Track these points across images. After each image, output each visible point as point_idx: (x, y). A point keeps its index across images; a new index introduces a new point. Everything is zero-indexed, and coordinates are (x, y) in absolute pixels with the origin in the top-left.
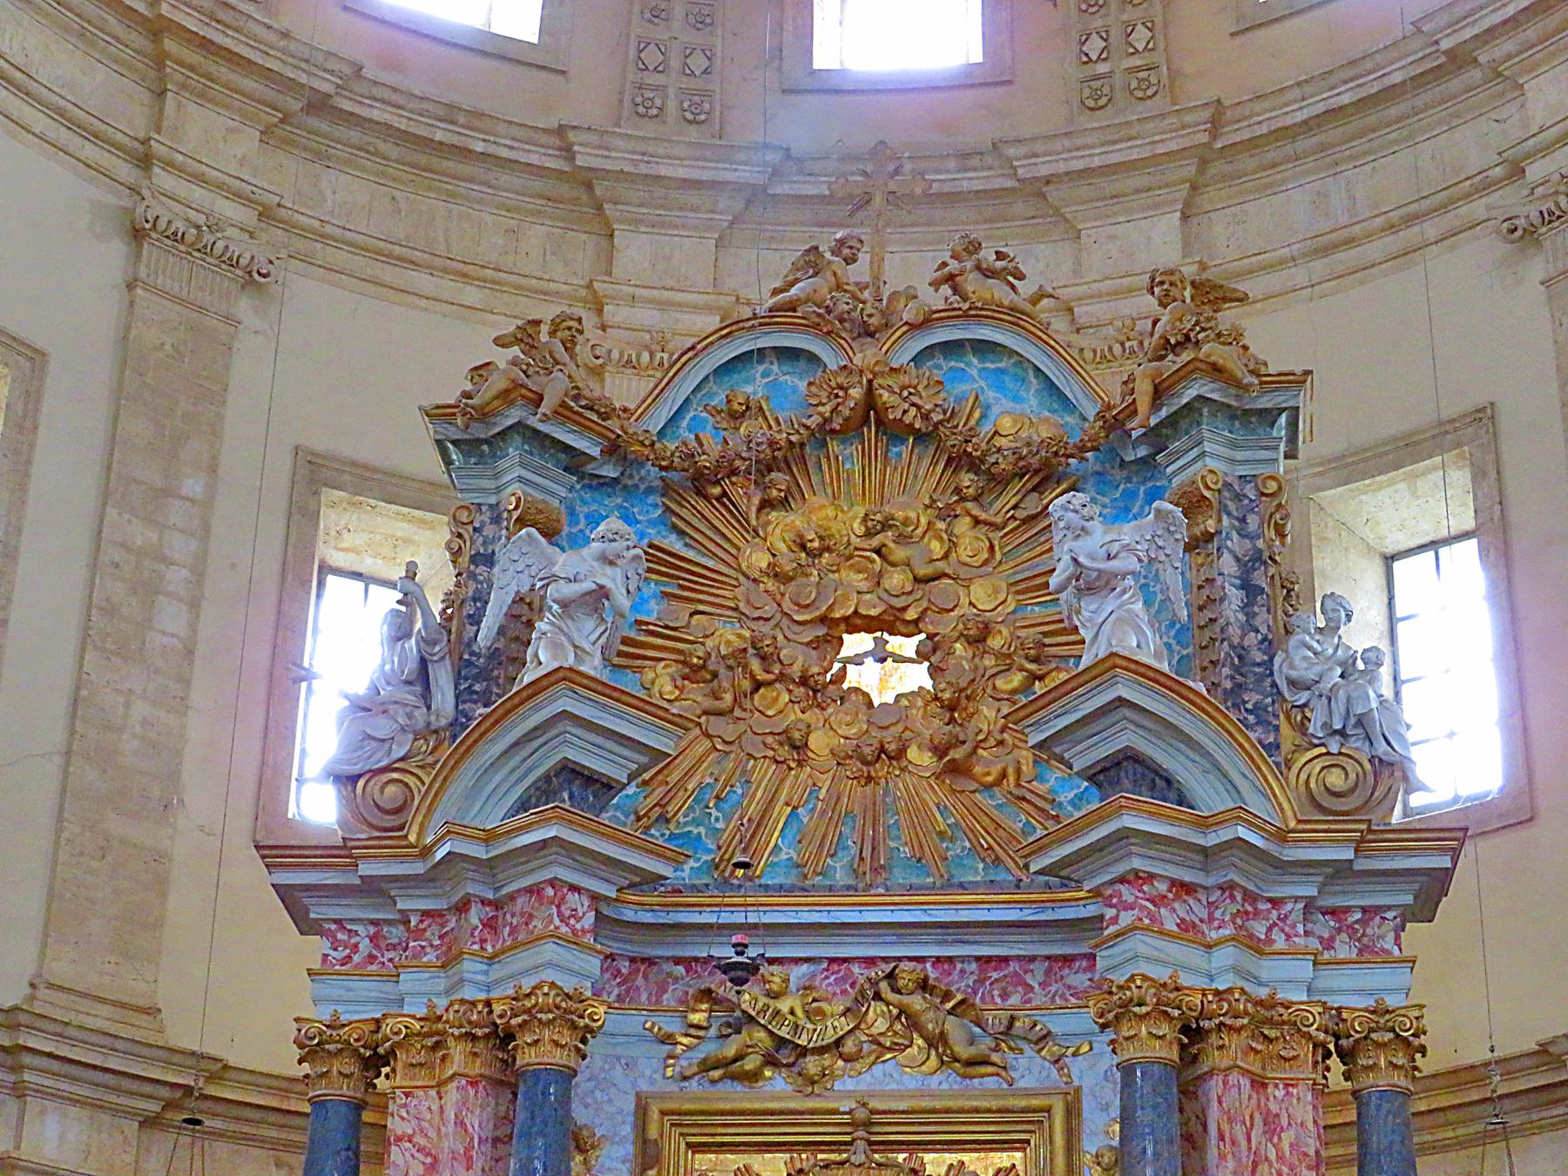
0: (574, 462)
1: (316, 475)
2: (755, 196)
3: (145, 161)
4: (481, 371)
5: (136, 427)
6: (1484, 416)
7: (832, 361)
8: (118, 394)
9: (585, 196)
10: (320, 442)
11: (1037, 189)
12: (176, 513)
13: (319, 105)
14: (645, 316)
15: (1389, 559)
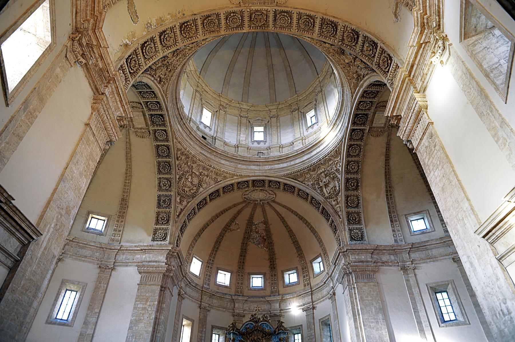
0: (236, 334)
1: (213, 327)
2: (246, 300)
3: (201, 302)
4: (229, 326)
5: (201, 325)
6: (301, 325)
7: (254, 324)
8: (199, 323)
9: (233, 301)
10: (213, 324)
11: (268, 301)
12: (203, 333)
13: (214, 295)
14: (238, 311)
15: (294, 334)
